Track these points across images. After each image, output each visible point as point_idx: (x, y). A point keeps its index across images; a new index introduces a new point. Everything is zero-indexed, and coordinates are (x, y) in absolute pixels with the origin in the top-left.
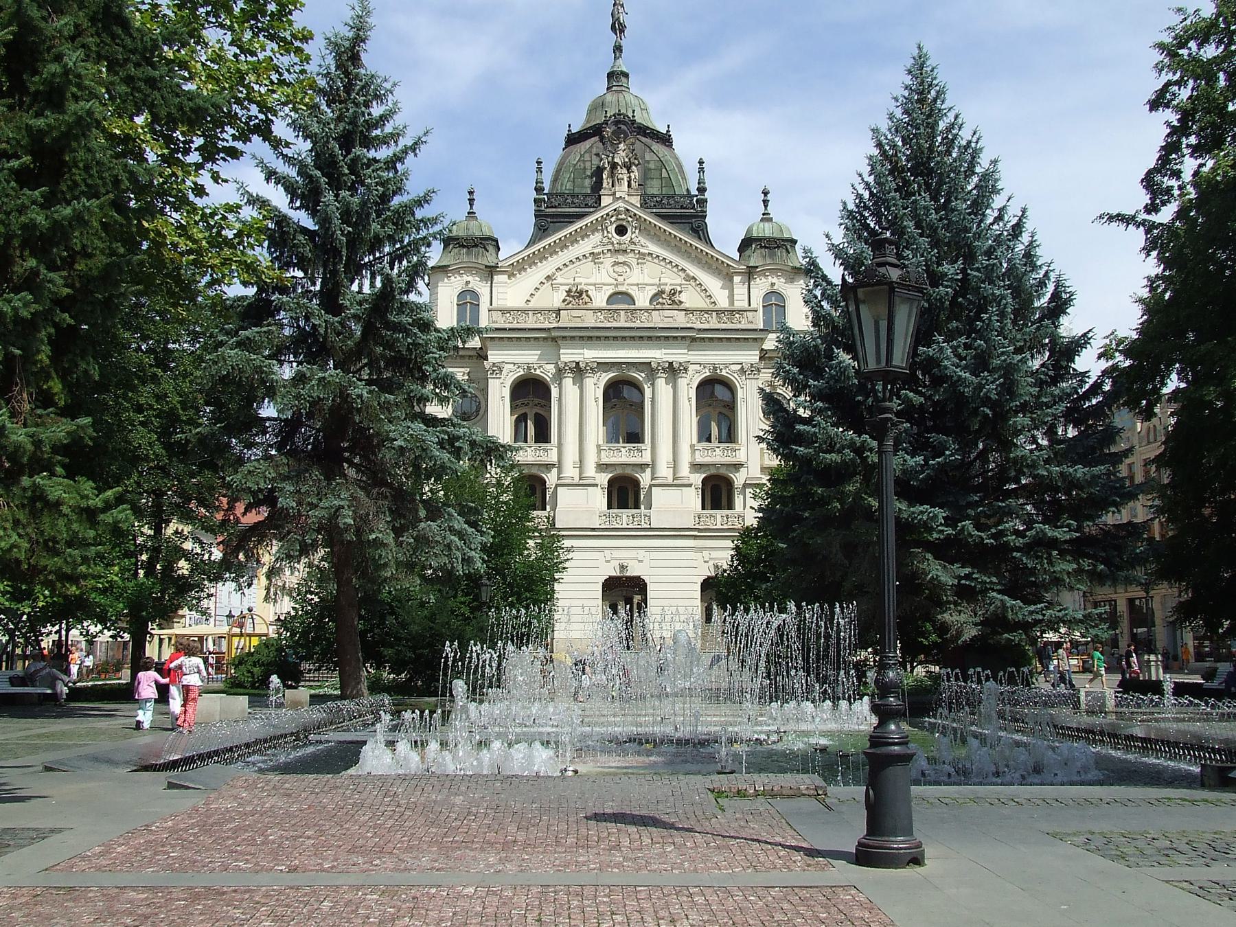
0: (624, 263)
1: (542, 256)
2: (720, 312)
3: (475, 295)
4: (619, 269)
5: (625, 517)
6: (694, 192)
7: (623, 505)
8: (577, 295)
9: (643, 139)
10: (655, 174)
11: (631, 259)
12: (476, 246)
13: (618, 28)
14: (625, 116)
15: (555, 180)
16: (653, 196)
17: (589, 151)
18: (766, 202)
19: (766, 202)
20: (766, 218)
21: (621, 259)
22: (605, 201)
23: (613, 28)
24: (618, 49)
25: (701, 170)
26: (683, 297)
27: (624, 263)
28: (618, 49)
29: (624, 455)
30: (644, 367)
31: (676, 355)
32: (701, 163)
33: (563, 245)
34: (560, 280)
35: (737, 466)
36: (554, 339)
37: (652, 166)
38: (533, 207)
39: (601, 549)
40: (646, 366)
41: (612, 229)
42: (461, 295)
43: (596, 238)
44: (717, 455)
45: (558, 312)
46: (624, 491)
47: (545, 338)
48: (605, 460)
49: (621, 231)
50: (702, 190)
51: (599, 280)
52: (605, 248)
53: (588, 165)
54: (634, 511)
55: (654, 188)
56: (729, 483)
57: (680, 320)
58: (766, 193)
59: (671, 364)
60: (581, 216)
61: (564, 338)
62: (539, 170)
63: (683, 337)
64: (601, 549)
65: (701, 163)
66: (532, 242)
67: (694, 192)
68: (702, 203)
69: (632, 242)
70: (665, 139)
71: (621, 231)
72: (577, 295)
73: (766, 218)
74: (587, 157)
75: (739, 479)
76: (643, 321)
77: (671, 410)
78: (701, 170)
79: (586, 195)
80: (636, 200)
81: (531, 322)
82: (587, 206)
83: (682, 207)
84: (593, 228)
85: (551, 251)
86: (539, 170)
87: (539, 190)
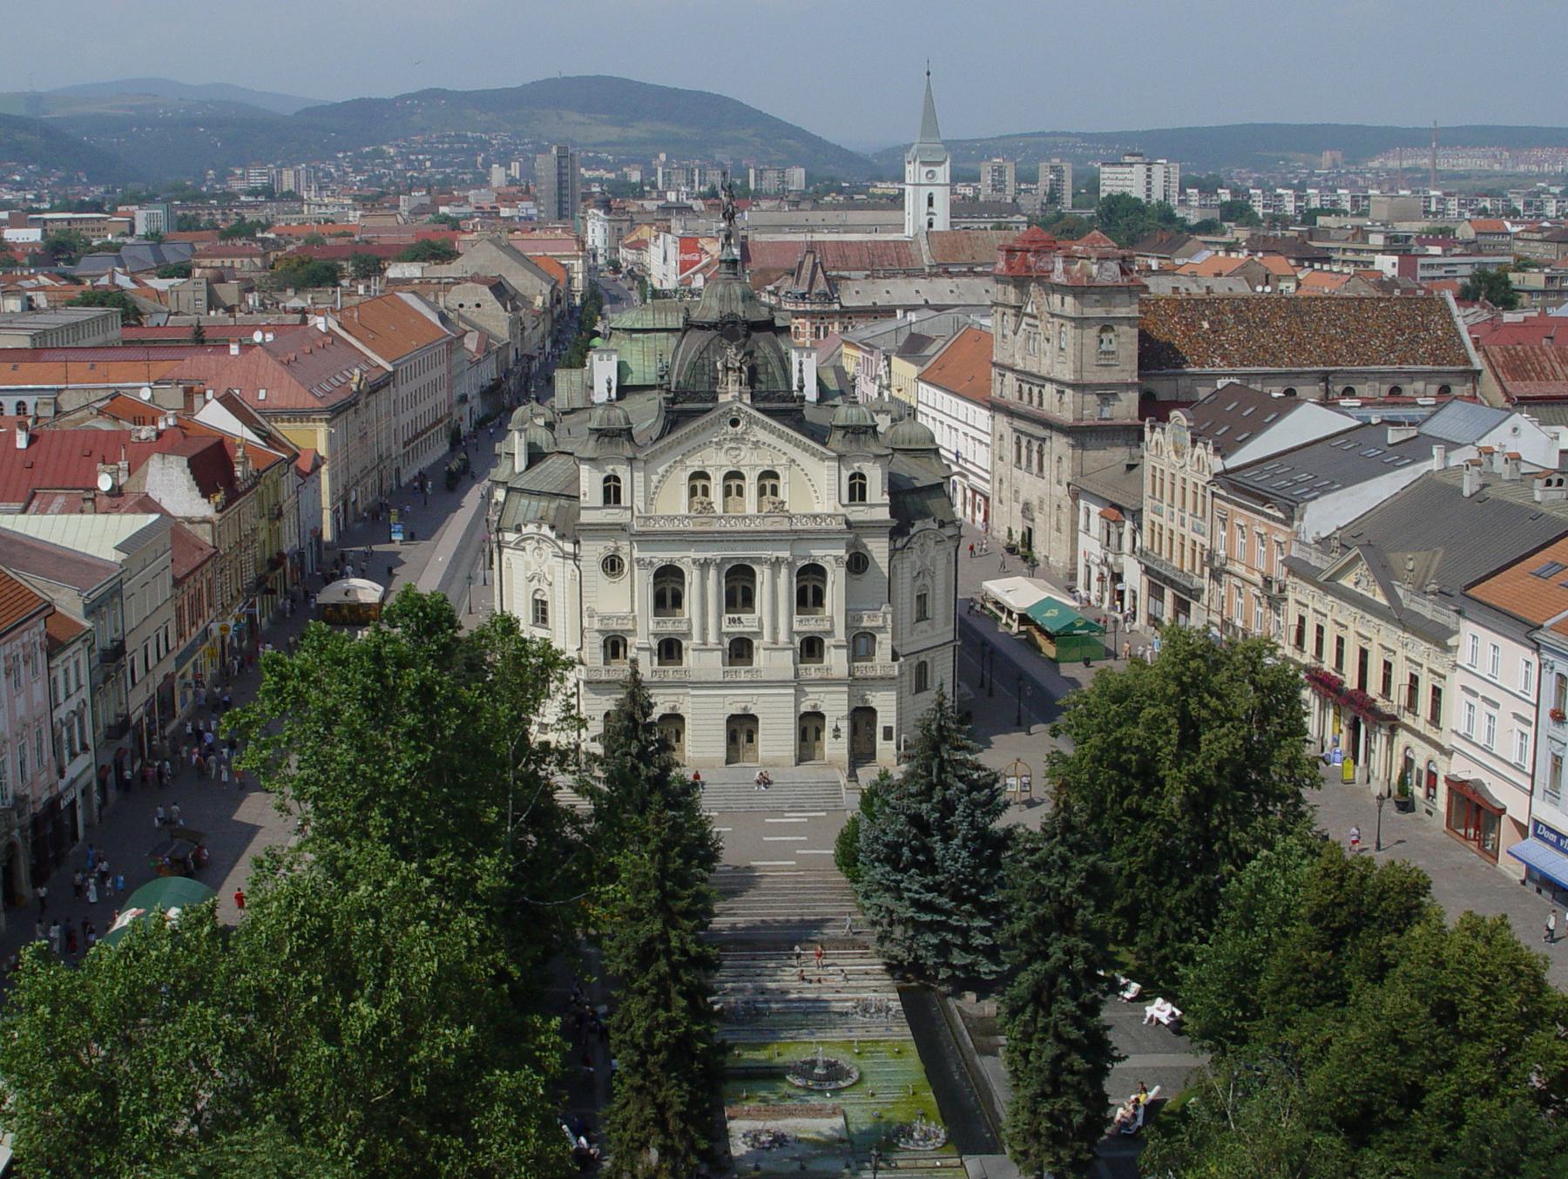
3: (617, 479)
4: (734, 453)
5: (742, 673)
6: (795, 388)
10: (761, 369)
12: (620, 435)
22: (722, 399)
40: (758, 560)
42: (607, 479)
44: (810, 625)
56: (822, 641)
67: (795, 388)
71: (735, 423)
75: (827, 642)
76: (757, 525)
80: (747, 399)
81: (669, 527)
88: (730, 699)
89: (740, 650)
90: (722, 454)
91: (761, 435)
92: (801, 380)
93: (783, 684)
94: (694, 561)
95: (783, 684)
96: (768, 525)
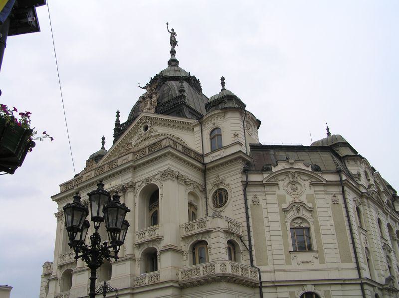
13: (174, 43)
24: (173, 52)
28: (173, 52)
35: (159, 240)
41: (142, 130)
52: (140, 140)
63: (128, 168)
71: (146, 128)
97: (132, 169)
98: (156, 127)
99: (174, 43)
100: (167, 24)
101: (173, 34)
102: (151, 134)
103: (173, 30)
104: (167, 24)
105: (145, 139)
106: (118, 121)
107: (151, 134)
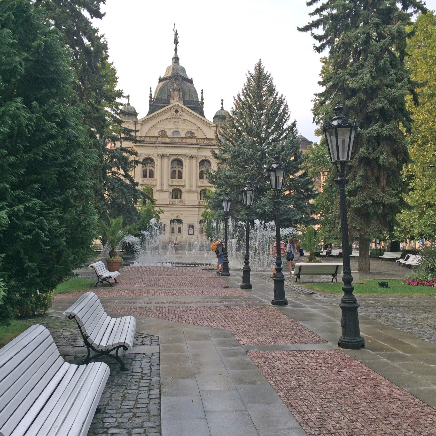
0: (178, 122)
1: (151, 119)
2: (207, 139)
4: (176, 124)
5: (177, 201)
6: (200, 100)
7: (176, 198)
8: (163, 134)
9: (184, 82)
11: (180, 121)
13: (176, 42)
14: (178, 74)
15: (155, 94)
16: (187, 101)
17: (167, 84)
18: (222, 104)
19: (222, 104)
20: (222, 109)
21: (176, 120)
22: (172, 101)
23: (174, 42)
24: (176, 50)
25: (202, 93)
26: (196, 135)
27: (178, 122)
28: (176, 50)
29: (177, 182)
30: (184, 156)
31: (194, 152)
32: (202, 90)
33: (158, 115)
34: (158, 127)
36: (156, 146)
37: (186, 91)
38: (148, 103)
39: (169, 211)
43: (169, 114)
45: (157, 137)
46: (176, 193)
47: (153, 146)
48: (170, 184)
49: (177, 111)
50: (202, 99)
51: (170, 128)
52: (172, 117)
53: (166, 89)
54: (180, 200)
55: (187, 98)
57: (195, 141)
58: (222, 100)
59: (192, 155)
60: (165, 106)
61: (159, 146)
62: (151, 91)
63: (196, 147)
64: (169, 211)
65: (202, 90)
66: (149, 114)
67: (200, 100)
68: (202, 103)
69: (180, 115)
70: (191, 81)
71: (177, 111)
72: (163, 134)
73: (222, 109)
74: (166, 87)
77: (191, 170)
78: (202, 93)
79: (166, 100)
80: (181, 102)
82: (166, 103)
83: (196, 105)
84: (168, 110)
85: (154, 117)
86: (151, 91)
87: (151, 97)
88: (172, 213)
89: (176, 193)
90: (171, 124)
91: (187, 117)
92: (202, 97)
93: (193, 206)
94: (159, 155)
95: (193, 206)
96: (188, 141)
97: (197, 149)
98: (184, 114)
99: (176, 42)
100: (174, 24)
101: (176, 34)
102: (180, 117)
103: (176, 31)
104: (174, 24)
105: (175, 118)
106: (151, 95)
107: (180, 117)
